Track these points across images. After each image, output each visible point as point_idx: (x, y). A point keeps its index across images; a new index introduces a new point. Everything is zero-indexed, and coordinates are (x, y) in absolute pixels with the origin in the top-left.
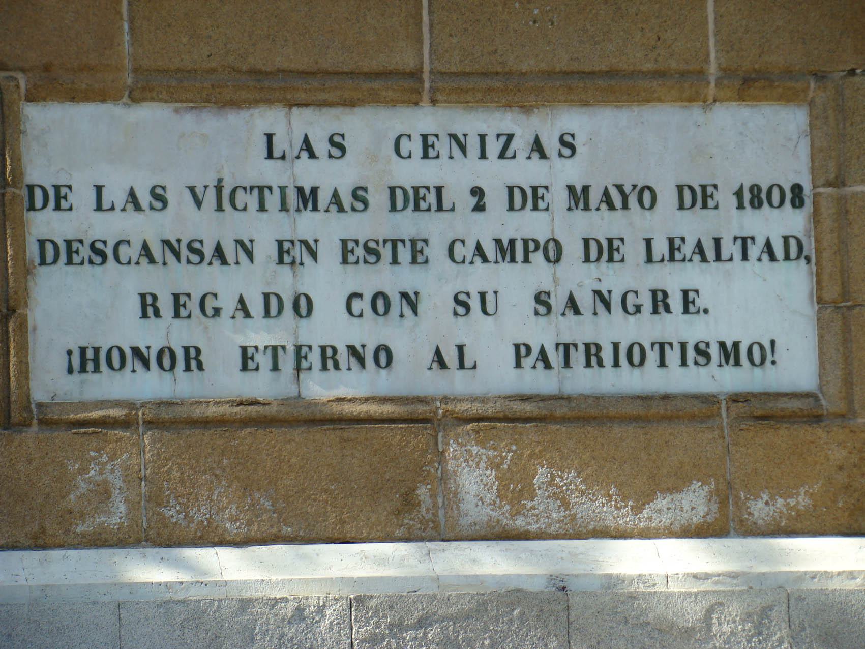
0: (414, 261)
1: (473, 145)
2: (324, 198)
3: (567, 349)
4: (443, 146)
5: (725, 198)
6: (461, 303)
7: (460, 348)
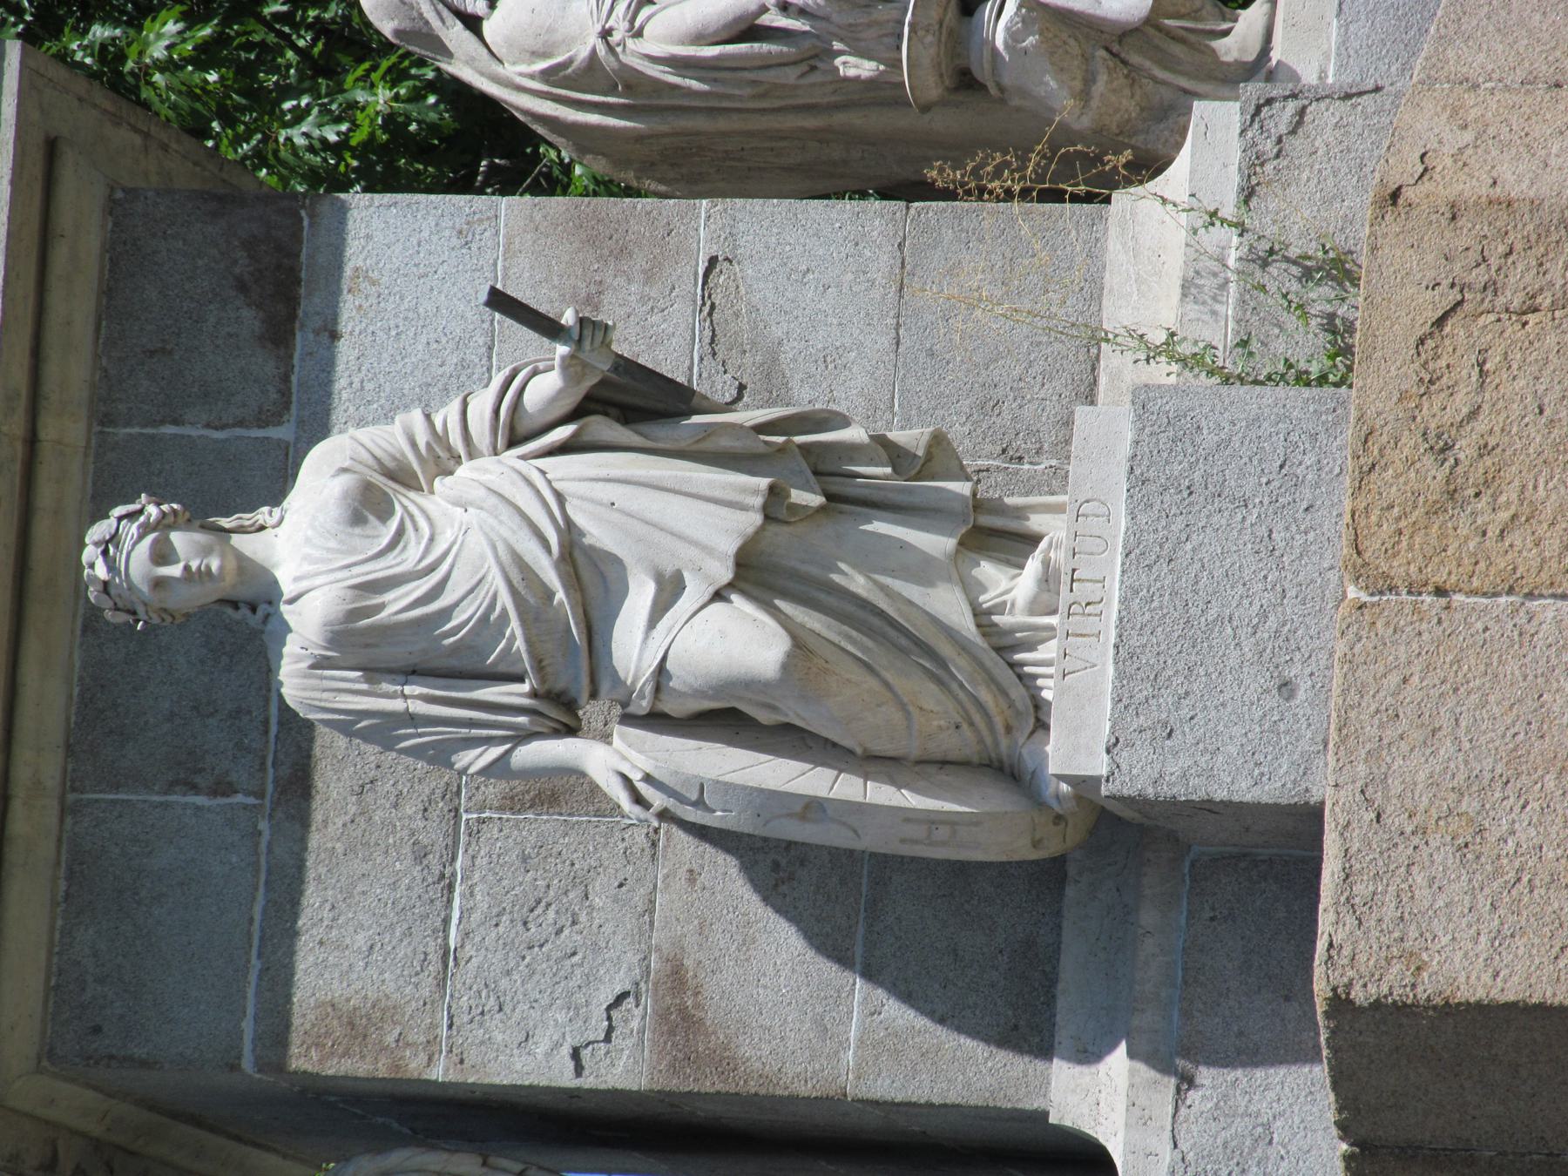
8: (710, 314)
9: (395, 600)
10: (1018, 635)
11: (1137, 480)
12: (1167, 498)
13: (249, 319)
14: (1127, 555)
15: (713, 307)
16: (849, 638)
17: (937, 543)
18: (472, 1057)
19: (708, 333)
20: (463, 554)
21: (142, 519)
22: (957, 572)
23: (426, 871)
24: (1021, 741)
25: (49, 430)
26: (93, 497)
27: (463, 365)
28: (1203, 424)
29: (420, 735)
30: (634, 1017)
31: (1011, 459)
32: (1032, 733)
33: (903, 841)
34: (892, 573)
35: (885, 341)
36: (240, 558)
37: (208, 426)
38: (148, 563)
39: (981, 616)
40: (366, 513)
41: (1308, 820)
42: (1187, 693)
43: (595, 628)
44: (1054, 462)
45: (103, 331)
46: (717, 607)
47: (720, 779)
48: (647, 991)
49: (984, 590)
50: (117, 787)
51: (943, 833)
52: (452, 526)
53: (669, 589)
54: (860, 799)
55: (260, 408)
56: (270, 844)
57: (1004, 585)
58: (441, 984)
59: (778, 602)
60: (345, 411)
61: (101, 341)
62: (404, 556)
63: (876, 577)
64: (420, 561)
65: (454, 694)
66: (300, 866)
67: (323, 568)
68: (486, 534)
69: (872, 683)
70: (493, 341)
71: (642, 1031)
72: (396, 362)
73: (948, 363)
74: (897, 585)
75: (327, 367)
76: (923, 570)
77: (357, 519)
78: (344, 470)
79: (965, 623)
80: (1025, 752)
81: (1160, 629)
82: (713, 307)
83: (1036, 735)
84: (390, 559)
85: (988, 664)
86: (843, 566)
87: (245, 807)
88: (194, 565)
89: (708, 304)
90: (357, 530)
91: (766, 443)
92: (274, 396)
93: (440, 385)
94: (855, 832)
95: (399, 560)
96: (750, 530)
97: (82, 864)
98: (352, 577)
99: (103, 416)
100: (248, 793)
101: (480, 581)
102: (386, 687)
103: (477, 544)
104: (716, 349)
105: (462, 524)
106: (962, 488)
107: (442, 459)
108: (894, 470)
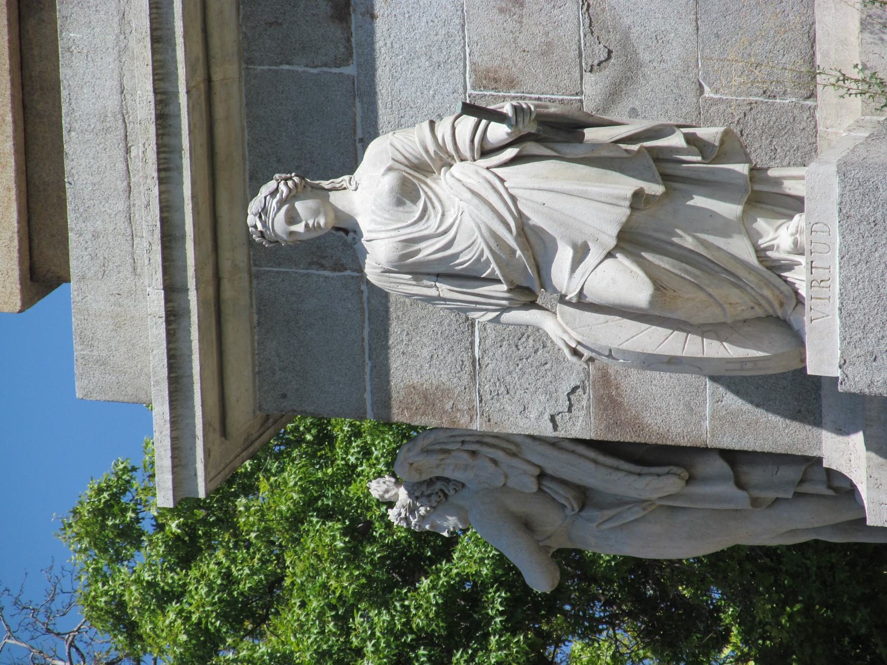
8: (588, 10)
9: (427, 247)
10: (782, 262)
11: (844, 217)
12: (862, 227)
14: (842, 258)
15: (589, 5)
16: (686, 272)
17: (730, 210)
18: (495, 418)
19: (587, 21)
20: (462, 227)
21: (278, 196)
22: (744, 227)
23: (458, 316)
24: (789, 312)
25: (228, 292)
26: (247, 105)
27: (448, 35)
28: (880, 186)
29: (446, 304)
30: (584, 400)
31: (769, 97)
32: (796, 305)
33: (727, 370)
34: (707, 232)
35: (691, 28)
36: (338, 213)
37: (307, 66)
38: (284, 224)
39: (760, 253)
40: (404, 199)
42: (883, 337)
43: (541, 267)
44: (794, 100)
45: (241, 11)
46: (609, 261)
47: (620, 347)
48: (589, 385)
49: (760, 236)
50: (279, 265)
51: (749, 365)
52: (454, 207)
53: (581, 252)
54: (700, 355)
55: (335, 56)
56: (368, 298)
57: (772, 235)
58: (473, 378)
59: (643, 254)
60: (384, 59)
61: (240, 17)
62: (429, 224)
63: (699, 235)
64: (438, 228)
65: (464, 290)
66: (387, 310)
67: (383, 228)
68: (474, 220)
69: (702, 296)
70: (464, 22)
71: (588, 407)
72: (410, 32)
73: (728, 41)
74: (711, 239)
75: (371, 34)
76: (725, 228)
77: (400, 203)
78: (390, 169)
79: (753, 259)
80: (792, 318)
81: (864, 300)
82: (589, 5)
83: (797, 308)
84: (421, 225)
85: (767, 276)
86: (678, 231)
87: (353, 277)
88: (311, 223)
89: (586, 4)
90: (401, 209)
91: (626, 151)
92: (342, 50)
93: (436, 46)
94: (699, 368)
95: (426, 226)
96: (624, 219)
97: (265, 306)
98: (400, 235)
99: (247, 59)
100: (353, 271)
101: (473, 243)
102: (425, 282)
103: (468, 223)
104: (593, 30)
105: (459, 207)
106: (742, 169)
108: (703, 158)
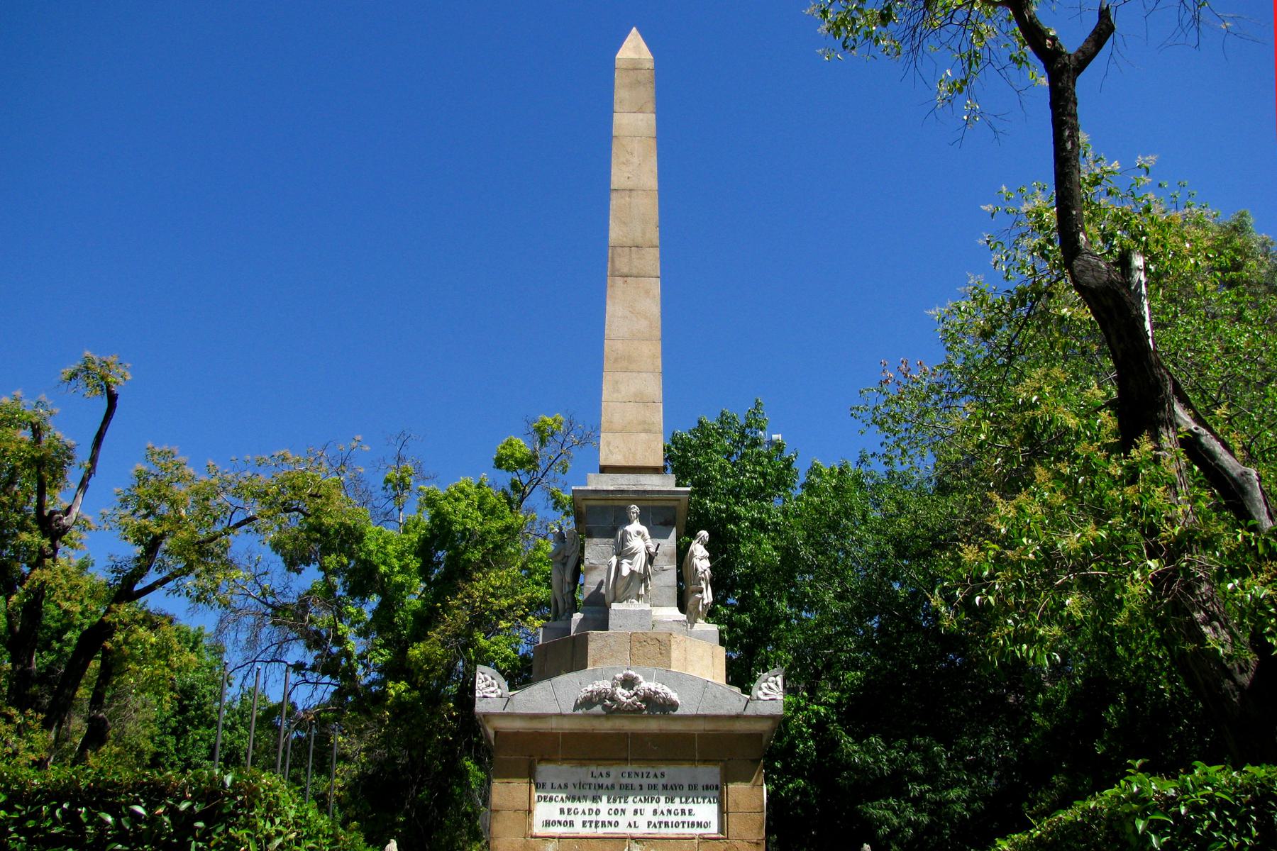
0: (625, 802)
1: (640, 776)
2: (604, 787)
3: (660, 823)
4: (633, 775)
5: (700, 788)
6: (636, 812)
7: (635, 823)
13: (662, 521)
41: (607, 629)
53: (631, 564)
99: (653, 507)
107: (645, 540)
